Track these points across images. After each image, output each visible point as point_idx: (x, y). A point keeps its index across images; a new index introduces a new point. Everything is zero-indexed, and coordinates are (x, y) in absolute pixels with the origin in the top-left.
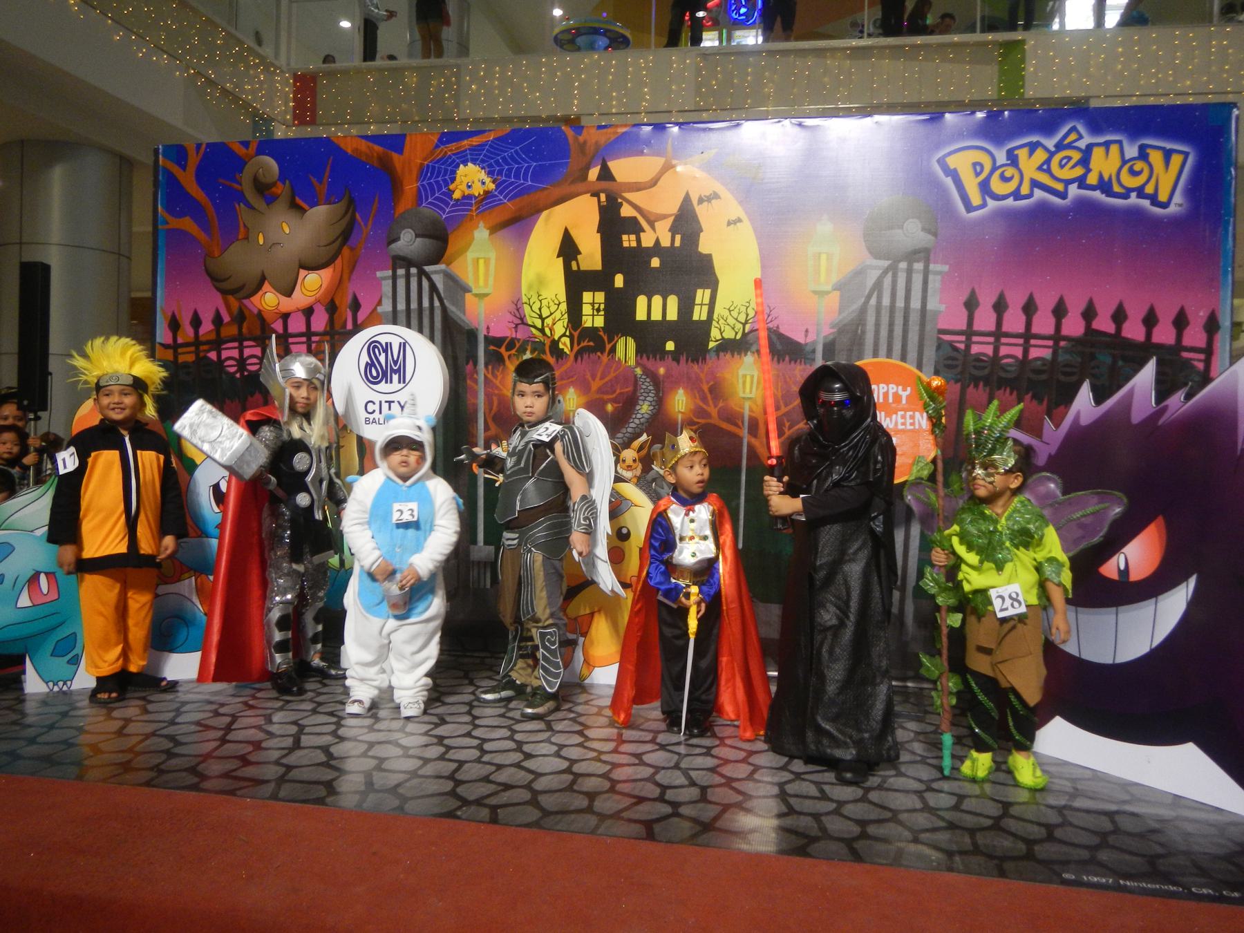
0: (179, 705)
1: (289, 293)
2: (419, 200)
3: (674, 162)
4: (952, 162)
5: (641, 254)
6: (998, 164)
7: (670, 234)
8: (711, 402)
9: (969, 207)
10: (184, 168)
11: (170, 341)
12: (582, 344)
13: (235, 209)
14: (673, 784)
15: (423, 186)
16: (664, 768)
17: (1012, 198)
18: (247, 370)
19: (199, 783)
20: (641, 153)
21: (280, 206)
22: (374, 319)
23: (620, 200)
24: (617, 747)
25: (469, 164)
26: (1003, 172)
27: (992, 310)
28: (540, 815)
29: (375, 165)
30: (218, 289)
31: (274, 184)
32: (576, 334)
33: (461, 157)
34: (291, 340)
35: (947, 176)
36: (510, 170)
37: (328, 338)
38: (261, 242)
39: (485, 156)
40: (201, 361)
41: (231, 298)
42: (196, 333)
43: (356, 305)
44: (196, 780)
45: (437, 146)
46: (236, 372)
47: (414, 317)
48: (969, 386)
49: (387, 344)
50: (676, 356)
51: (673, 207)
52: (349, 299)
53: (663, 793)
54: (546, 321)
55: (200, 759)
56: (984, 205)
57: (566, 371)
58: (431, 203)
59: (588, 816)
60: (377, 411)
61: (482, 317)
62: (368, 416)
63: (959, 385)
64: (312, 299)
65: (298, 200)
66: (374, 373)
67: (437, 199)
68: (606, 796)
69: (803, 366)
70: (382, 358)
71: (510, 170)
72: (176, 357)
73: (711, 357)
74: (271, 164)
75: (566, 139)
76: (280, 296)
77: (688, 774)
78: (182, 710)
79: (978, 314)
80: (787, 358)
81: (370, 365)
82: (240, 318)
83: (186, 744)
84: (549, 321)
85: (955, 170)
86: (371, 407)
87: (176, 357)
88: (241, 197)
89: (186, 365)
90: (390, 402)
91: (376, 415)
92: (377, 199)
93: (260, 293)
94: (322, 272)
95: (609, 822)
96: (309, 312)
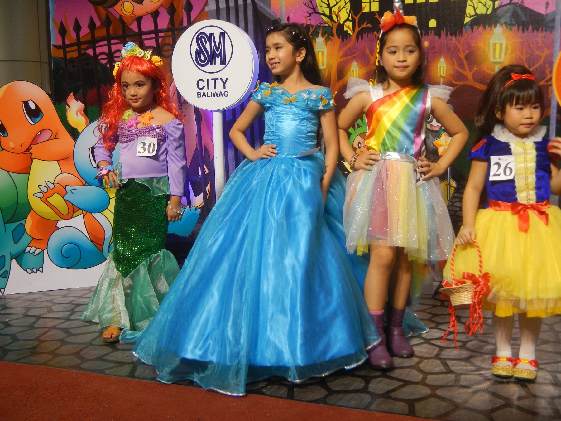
0: (74, 306)
8: (467, 68)
11: (60, 43)
12: (362, 26)
14: (433, 372)
16: (427, 358)
19: (80, 364)
22: (202, 16)
28: (326, 393)
32: (357, 18)
34: (144, 37)
37: (170, 33)
40: (83, 56)
41: (100, 8)
42: (78, 36)
43: (189, 7)
44: (79, 361)
46: (107, 64)
47: (232, 12)
49: (210, 34)
50: (437, 31)
52: (184, 2)
53: (424, 379)
54: (333, 9)
55: (84, 346)
57: (350, 49)
59: (363, 395)
60: (206, 87)
61: (284, 9)
62: (200, 91)
66: (203, 58)
68: (380, 379)
69: (543, 34)
70: (208, 46)
72: (65, 55)
73: (467, 31)
76: (134, 4)
77: (446, 363)
78: (76, 310)
80: (531, 28)
81: (198, 52)
82: (108, 22)
83: (75, 335)
84: (335, 9)
86: (201, 84)
87: (65, 55)
89: (72, 61)
90: (215, 80)
91: (205, 90)
95: (381, 399)
96: (155, 14)
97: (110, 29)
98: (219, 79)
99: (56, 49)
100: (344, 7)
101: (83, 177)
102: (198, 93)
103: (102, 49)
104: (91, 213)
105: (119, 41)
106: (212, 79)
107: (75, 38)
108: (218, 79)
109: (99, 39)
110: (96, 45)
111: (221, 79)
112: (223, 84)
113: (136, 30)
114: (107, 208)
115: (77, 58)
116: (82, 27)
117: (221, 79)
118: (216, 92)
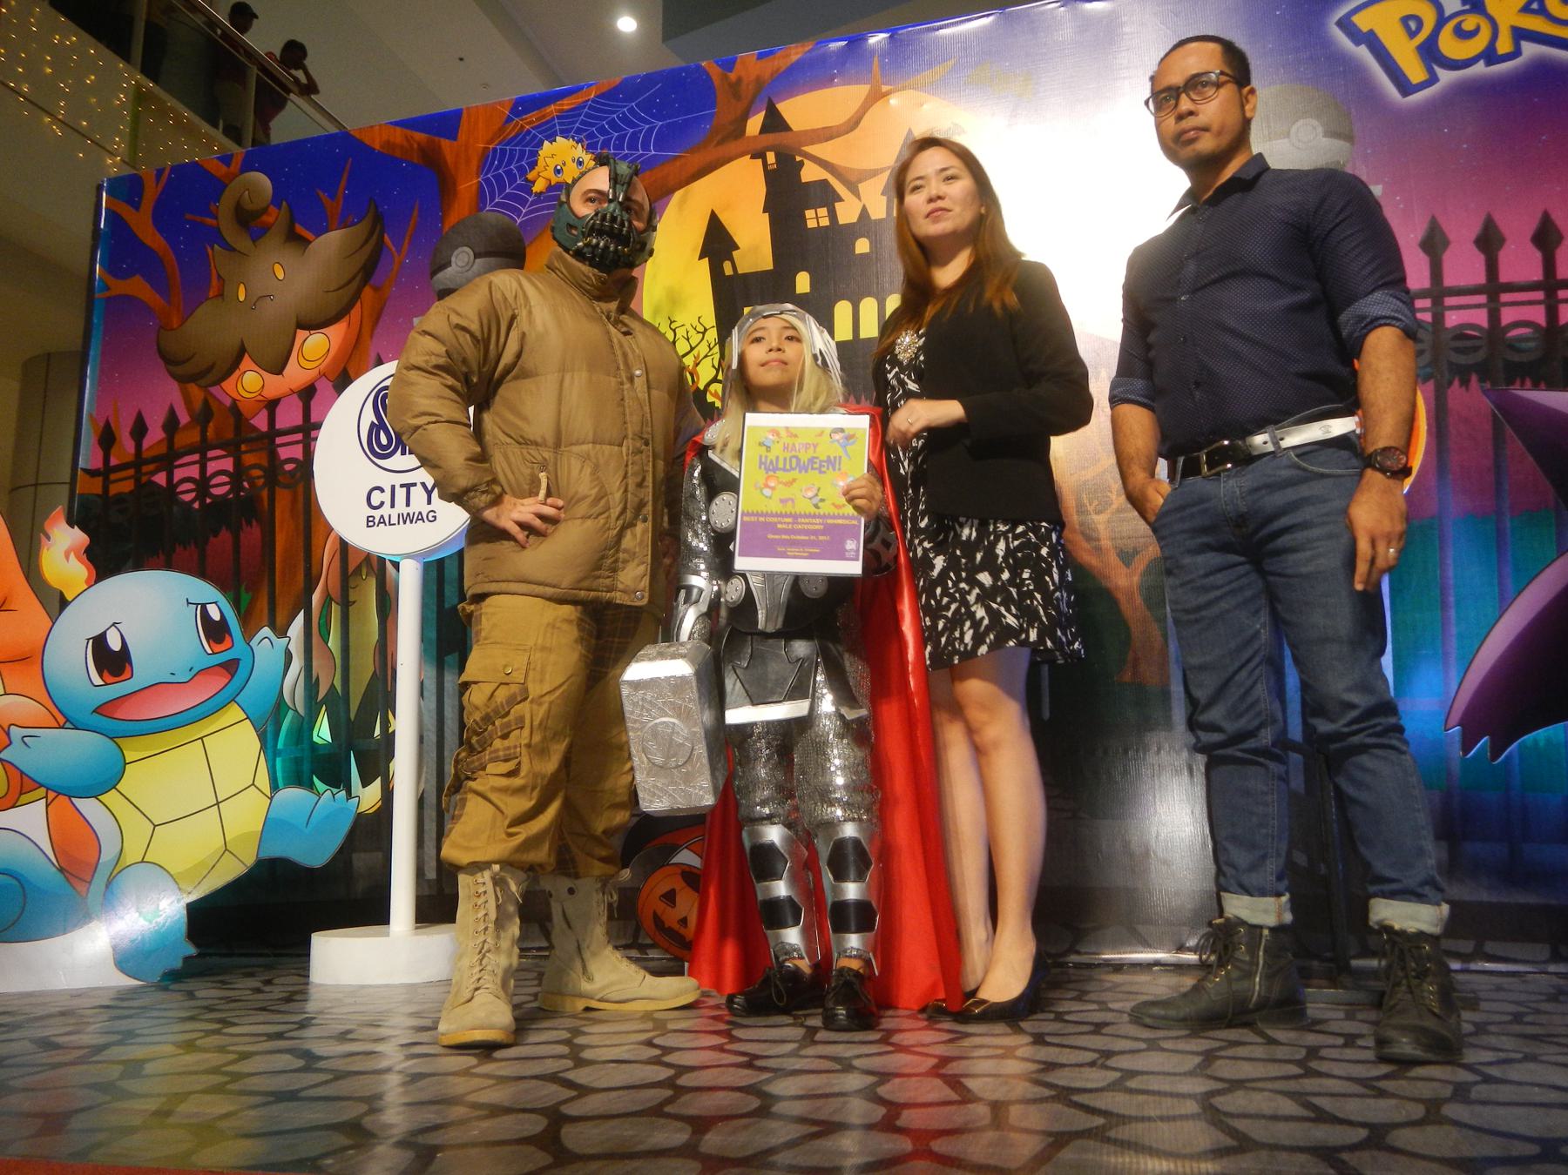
1: (279, 370)
2: (481, 200)
3: (885, 88)
4: (1363, 21)
5: (840, 235)
6: (1448, 13)
7: (885, 198)
9: (1405, 87)
10: (137, 206)
11: (99, 465)
13: (208, 255)
14: (921, 1100)
15: (487, 181)
17: (1481, 63)
18: (211, 496)
20: (828, 82)
21: (272, 241)
23: (798, 159)
24: (799, 1049)
25: (558, 138)
26: (1460, 23)
27: (1475, 250)
29: (415, 161)
30: (172, 375)
31: (265, 211)
33: (545, 131)
34: (278, 440)
35: (1357, 43)
36: (621, 139)
38: (242, 298)
39: (583, 123)
40: (144, 489)
42: (138, 446)
45: (509, 120)
46: (193, 501)
48: (1450, 383)
51: (888, 156)
56: (1433, 79)
58: (498, 205)
60: (388, 503)
63: (1432, 381)
64: (317, 370)
65: (300, 229)
66: (384, 441)
67: (508, 197)
71: (621, 139)
74: (262, 182)
75: (712, 83)
79: (1449, 259)
81: (376, 428)
85: (1371, 32)
86: (377, 498)
87: (106, 489)
88: (217, 237)
89: (120, 498)
90: (408, 486)
91: (386, 511)
92: (417, 207)
93: (237, 372)
94: (331, 330)
96: (307, 393)
97: (209, 429)
98: (418, 485)
99: (88, 477)
100: (706, 356)
101: (62, 709)
102: (368, 517)
103: (187, 470)
104: (70, 797)
105: (224, 453)
106: (402, 486)
107: (133, 451)
108: (415, 485)
109: (182, 450)
110: (177, 463)
111: (423, 484)
112: (425, 496)
113: (264, 427)
114: (114, 787)
115: (131, 492)
116: (150, 428)
117: (423, 484)
118: (408, 514)
